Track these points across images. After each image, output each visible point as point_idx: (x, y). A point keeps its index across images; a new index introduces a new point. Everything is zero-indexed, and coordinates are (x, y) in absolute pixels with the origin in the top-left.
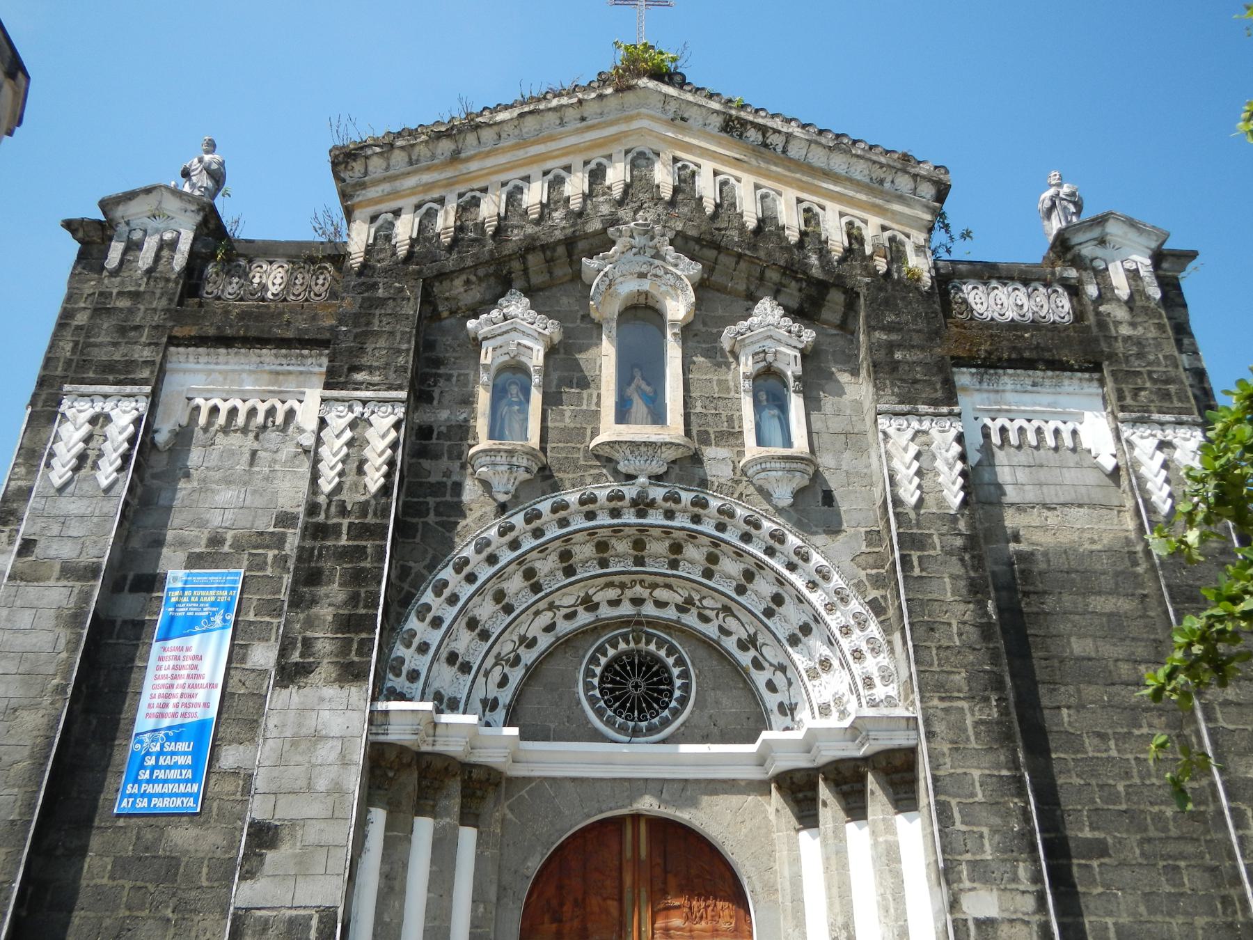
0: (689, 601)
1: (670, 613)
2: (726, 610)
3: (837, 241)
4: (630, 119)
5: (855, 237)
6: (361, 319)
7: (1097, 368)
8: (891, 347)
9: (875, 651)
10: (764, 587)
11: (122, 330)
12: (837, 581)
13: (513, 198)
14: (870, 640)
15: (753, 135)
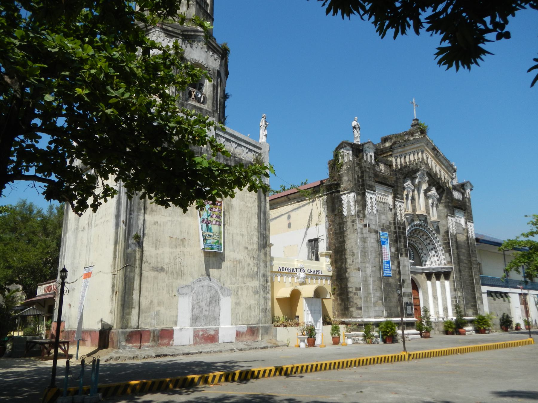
0: (416, 241)
1: (412, 242)
2: (420, 243)
3: (443, 179)
4: (422, 142)
5: (445, 179)
6: (396, 182)
7: (465, 210)
8: (449, 202)
9: (443, 255)
10: (428, 241)
11: (370, 177)
12: (440, 243)
13: (409, 158)
14: (443, 254)
15: (436, 152)
